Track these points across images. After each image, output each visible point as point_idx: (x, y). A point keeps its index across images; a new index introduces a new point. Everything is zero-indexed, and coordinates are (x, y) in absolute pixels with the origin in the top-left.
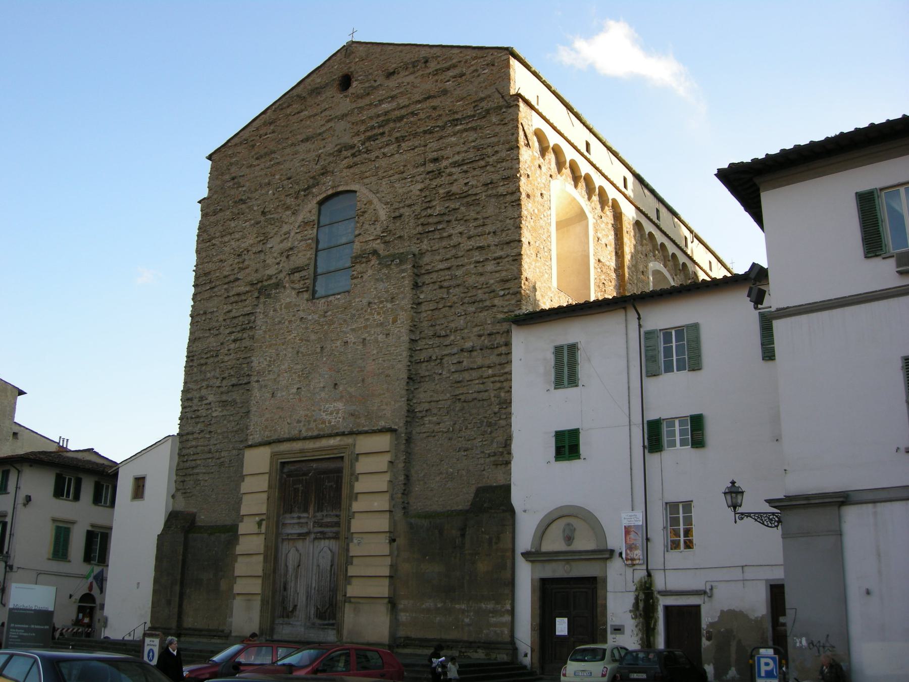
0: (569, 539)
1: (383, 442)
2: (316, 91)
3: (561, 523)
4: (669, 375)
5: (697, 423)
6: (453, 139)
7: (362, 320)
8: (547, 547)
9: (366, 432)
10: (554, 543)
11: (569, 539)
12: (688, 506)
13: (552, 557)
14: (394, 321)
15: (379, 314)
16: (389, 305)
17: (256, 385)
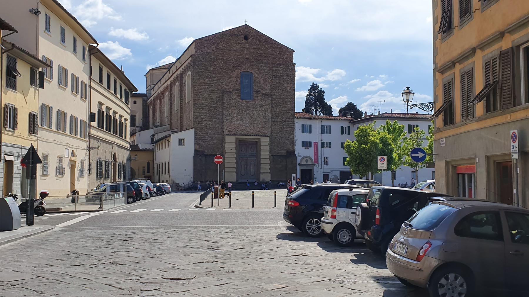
0: (307, 162)
1: (267, 139)
2: (237, 35)
3: (305, 159)
4: (327, 134)
5: (330, 143)
6: (280, 69)
7: (258, 109)
8: (302, 163)
9: (264, 136)
10: (304, 162)
11: (307, 162)
12: (327, 158)
13: (304, 165)
14: (267, 111)
15: (263, 108)
16: (266, 107)
17: (225, 119)
